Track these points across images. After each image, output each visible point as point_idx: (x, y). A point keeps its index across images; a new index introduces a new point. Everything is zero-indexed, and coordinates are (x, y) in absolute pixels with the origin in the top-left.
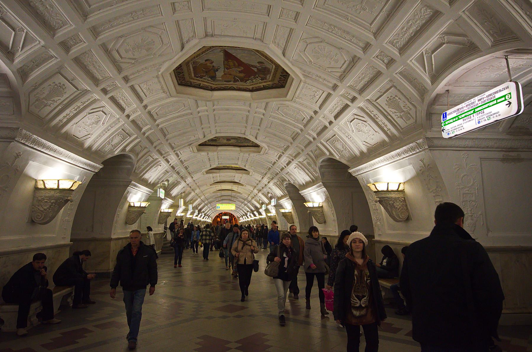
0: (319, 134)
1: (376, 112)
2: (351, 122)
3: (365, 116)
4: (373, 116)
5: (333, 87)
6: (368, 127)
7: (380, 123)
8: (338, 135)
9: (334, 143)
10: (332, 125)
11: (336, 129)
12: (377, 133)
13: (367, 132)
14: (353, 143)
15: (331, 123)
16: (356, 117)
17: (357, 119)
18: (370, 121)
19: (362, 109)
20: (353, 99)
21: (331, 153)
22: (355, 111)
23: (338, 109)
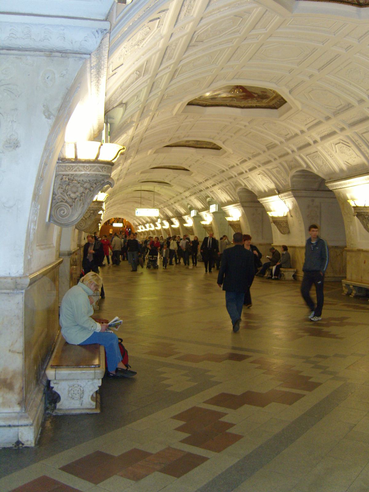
0: (300, 149)
1: (360, 141)
2: (336, 144)
3: (350, 142)
4: (357, 144)
5: (326, 118)
6: (351, 151)
7: (363, 150)
8: (321, 153)
9: (314, 158)
10: (316, 144)
11: (319, 148)
12: (359, 158)
13: (349, 154)
14: (334, 161)
15: (315, 142)
16: (341, 141)
17: (342, 143)
18: (353, 147)
19: (348, 137)
20: (342, 129)
21: (308, 166)
22: (341, 137)
23: (326, 133)
